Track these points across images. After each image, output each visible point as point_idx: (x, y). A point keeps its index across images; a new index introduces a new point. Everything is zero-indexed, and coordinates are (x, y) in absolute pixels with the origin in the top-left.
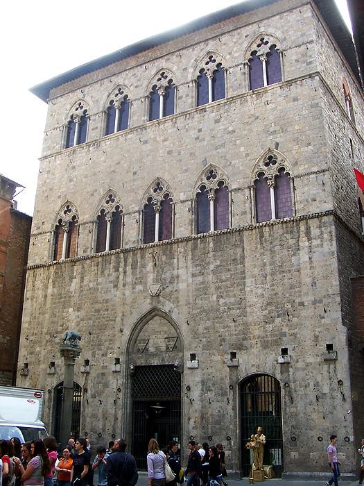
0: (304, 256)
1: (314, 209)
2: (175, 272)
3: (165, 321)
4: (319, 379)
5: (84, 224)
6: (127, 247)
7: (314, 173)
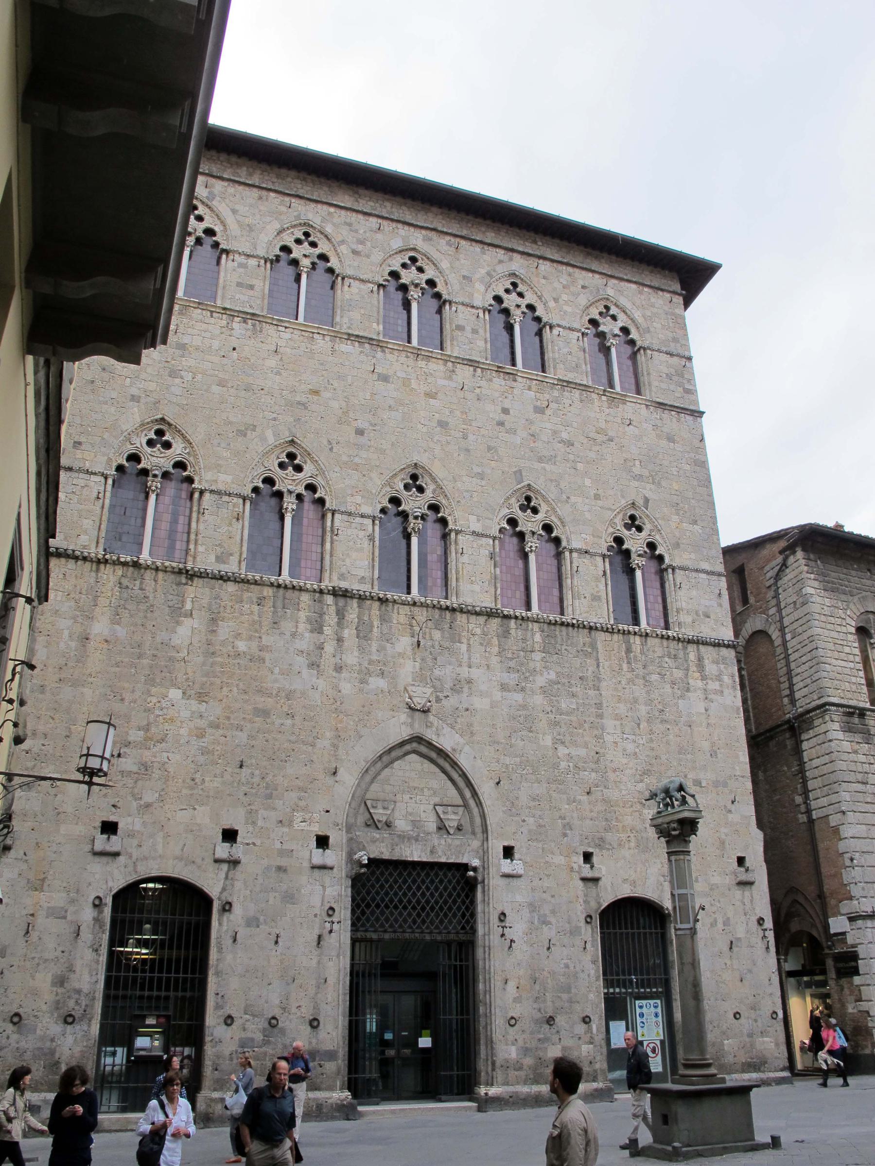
0: (695, 704)
1: (707, 631)
2: (464, 672)
4: (730, 914)
5: (219, 493)
6: (344, 585)
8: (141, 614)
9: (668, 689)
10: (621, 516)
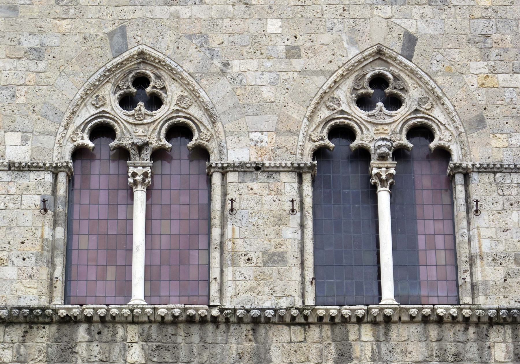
10: (349, 83)
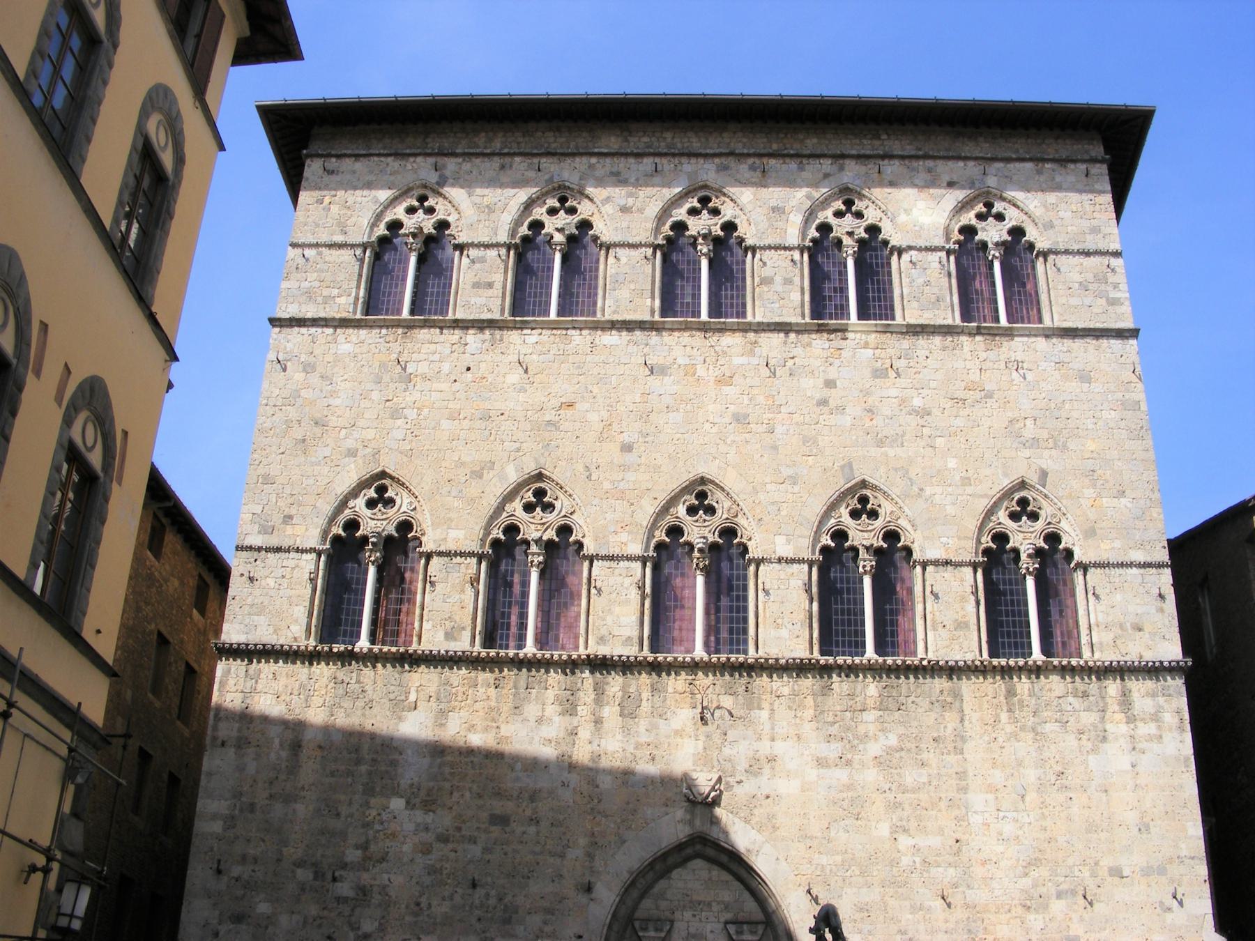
0: (1116, 758)
2: (765, 748)
3: (726, 876)
5: (448, 554)
6: (603, 651)
7: (1131, 565)
8: (359, 713)
9: (1071, 741)
